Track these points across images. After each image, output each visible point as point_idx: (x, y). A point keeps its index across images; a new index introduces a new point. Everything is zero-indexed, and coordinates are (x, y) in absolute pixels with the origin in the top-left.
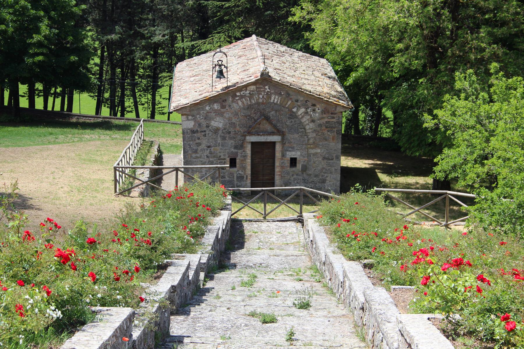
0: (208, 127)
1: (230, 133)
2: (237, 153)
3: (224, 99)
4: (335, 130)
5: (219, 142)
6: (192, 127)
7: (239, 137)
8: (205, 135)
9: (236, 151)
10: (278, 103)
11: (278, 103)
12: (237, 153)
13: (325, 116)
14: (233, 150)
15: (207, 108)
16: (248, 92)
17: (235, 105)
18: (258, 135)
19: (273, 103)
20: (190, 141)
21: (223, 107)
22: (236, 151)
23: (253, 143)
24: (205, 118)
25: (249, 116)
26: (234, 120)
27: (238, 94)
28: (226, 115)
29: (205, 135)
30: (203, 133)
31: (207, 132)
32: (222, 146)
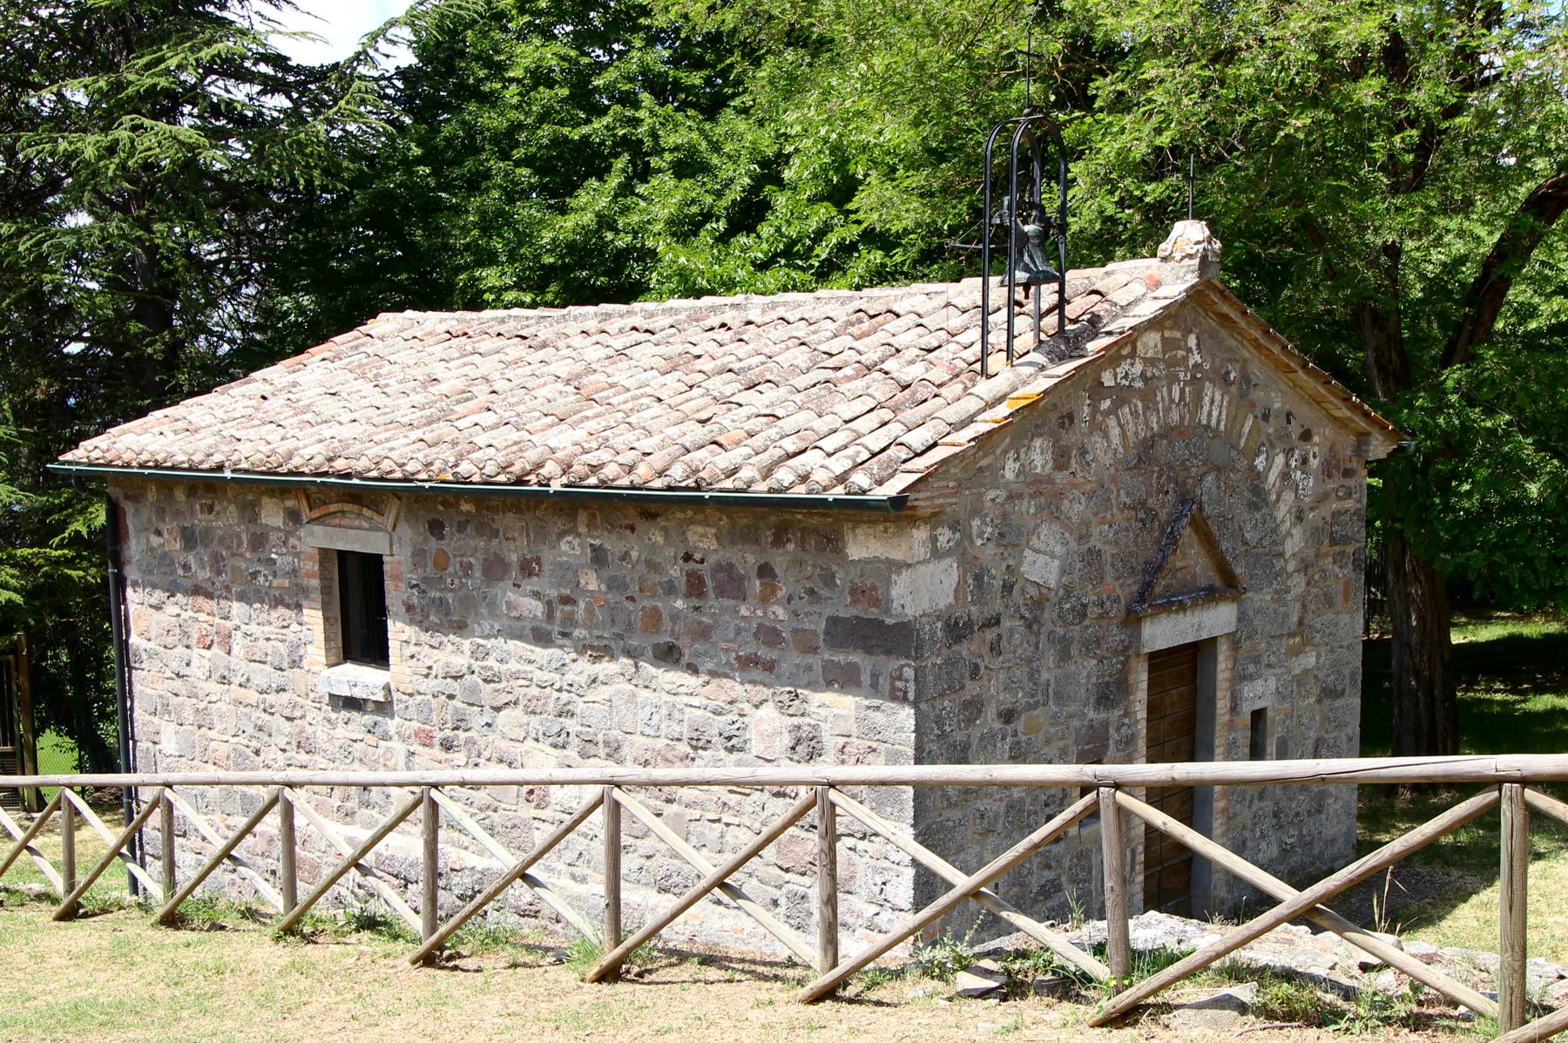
0: (1008, 588)
1: (1082, 613)
2: (1105, 725)
3: (1065, 411)
4: (1350, 549)
5: (1045, 676)
6: (951, 599)
7: (1116, 636)
8: (995, 648)
9: (1103, 715)
10: (1222, 427)
11: (1222, 427)
12: (1105, 725)
13: (1331, 485)
14: (1091, 714)
15: (1010, 470)
16: (1138, 368)
17: (1098, 441)
18: (1182, 608)
19: (1208, 426)
20: (942, 695)
21: (1061, 459)
22: (1103, 715)
23: (1158, 660)
24: (1001, 535)
25: (1143, 504)
26: (1095, 542)
27: (1107, 379)
28: (1076, 509)
29: (995, 648)
30: (990, 635)
31: (1006, 623)
32: (1060, 698)
